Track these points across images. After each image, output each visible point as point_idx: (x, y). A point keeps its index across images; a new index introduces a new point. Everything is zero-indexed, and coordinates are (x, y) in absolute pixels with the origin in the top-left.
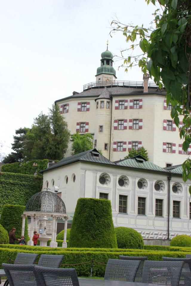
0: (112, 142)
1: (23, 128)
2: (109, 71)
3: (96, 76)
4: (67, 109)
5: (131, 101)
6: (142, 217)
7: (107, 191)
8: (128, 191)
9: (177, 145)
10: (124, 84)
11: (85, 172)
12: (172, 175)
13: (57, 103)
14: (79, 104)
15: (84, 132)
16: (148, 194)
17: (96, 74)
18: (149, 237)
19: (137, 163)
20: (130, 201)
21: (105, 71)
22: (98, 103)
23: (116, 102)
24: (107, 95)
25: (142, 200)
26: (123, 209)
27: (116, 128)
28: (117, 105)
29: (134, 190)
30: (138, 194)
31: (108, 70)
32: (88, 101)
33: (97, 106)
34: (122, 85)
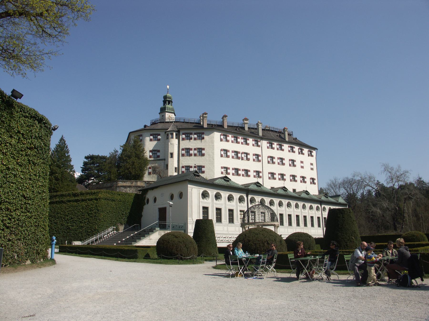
0: (181, 166)
1: (91, 154)
2: (170, 110)
3: (159, 113)
4: (140, 139)
5: (195, 134)
6: (231, 224)
7: (207, 205)
8: (222, 204)
9: (231, 169)
10: (184, 120)
11: (192, 190)
12: (250, 191)
13: (131, 134)
14: (151, 135)
15: (156, 158)
16: (234, 207)
17: (159, 112)
18: (220, 240)
19: (225, 182)
20: (223, 212)
21: (167, 110)
22: (168, 135)
23: (183, 134)
24: (175, 129)
25: (231, 211)
26: (219, 220)
27: (183, 155)
28: (184, 136)
29: (226, 204)
30: (228, 207)
31: (170, 108)
32: (158, 133)
33: (167, 137)
34: (183, 121)
